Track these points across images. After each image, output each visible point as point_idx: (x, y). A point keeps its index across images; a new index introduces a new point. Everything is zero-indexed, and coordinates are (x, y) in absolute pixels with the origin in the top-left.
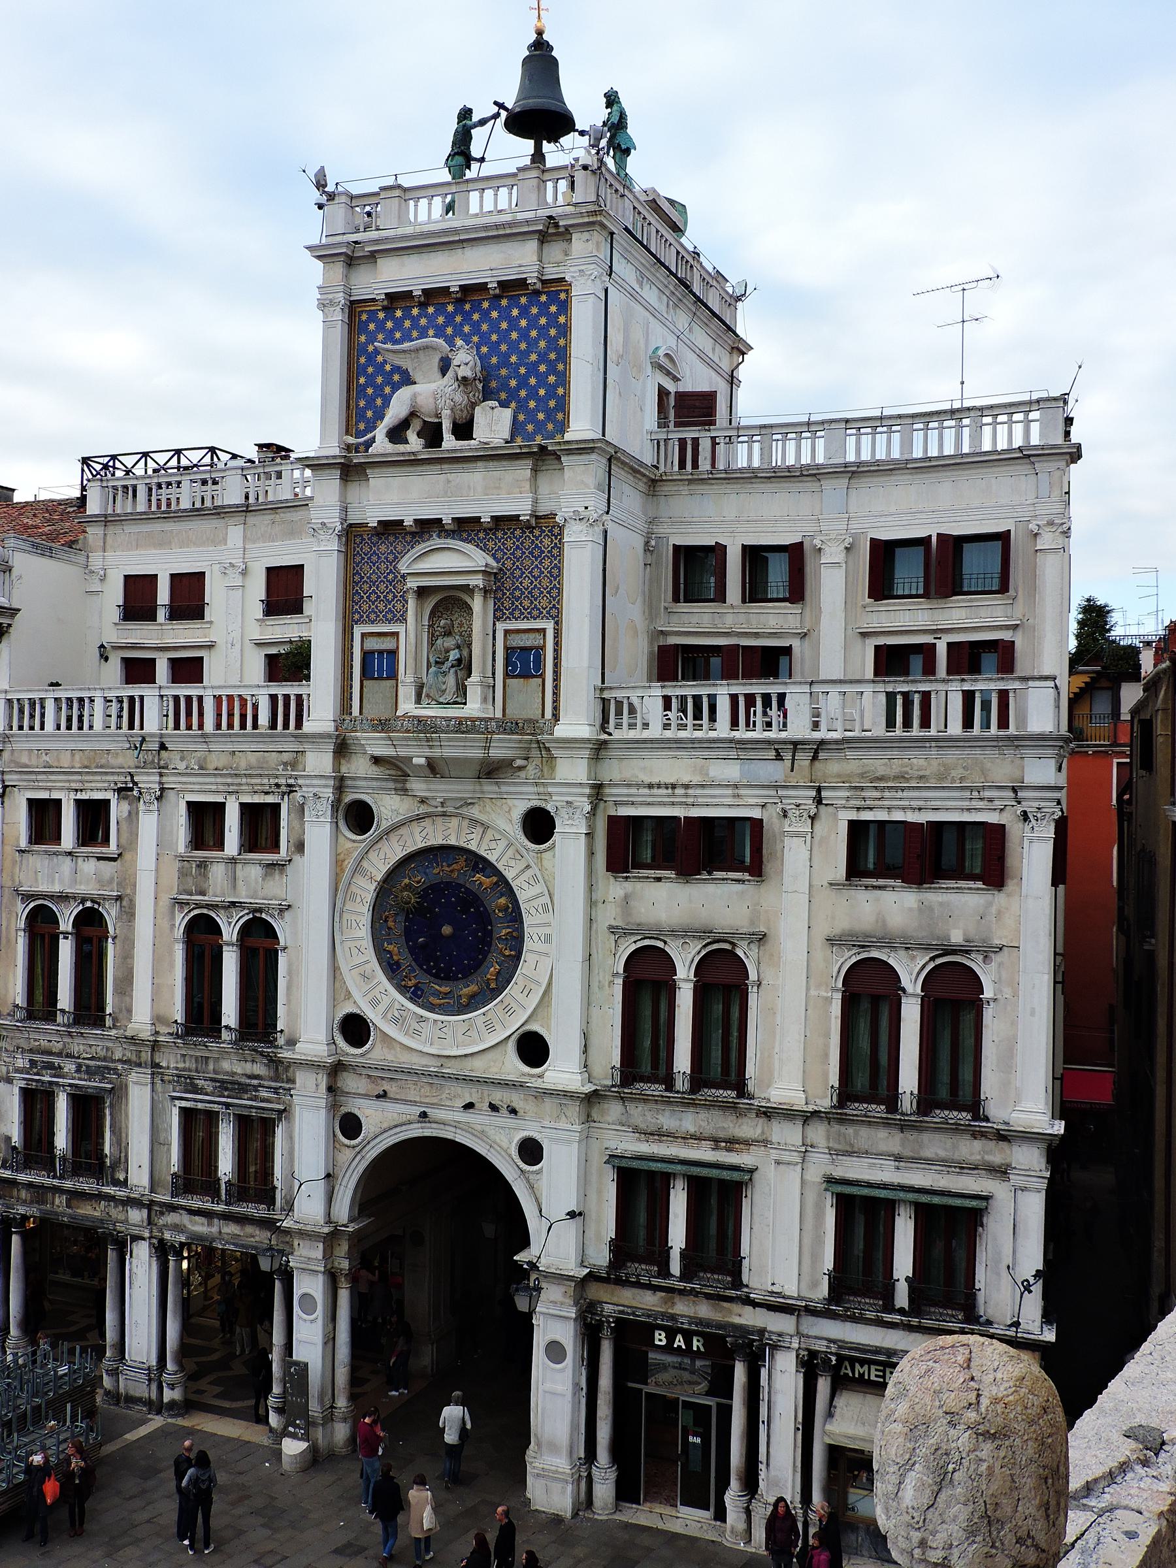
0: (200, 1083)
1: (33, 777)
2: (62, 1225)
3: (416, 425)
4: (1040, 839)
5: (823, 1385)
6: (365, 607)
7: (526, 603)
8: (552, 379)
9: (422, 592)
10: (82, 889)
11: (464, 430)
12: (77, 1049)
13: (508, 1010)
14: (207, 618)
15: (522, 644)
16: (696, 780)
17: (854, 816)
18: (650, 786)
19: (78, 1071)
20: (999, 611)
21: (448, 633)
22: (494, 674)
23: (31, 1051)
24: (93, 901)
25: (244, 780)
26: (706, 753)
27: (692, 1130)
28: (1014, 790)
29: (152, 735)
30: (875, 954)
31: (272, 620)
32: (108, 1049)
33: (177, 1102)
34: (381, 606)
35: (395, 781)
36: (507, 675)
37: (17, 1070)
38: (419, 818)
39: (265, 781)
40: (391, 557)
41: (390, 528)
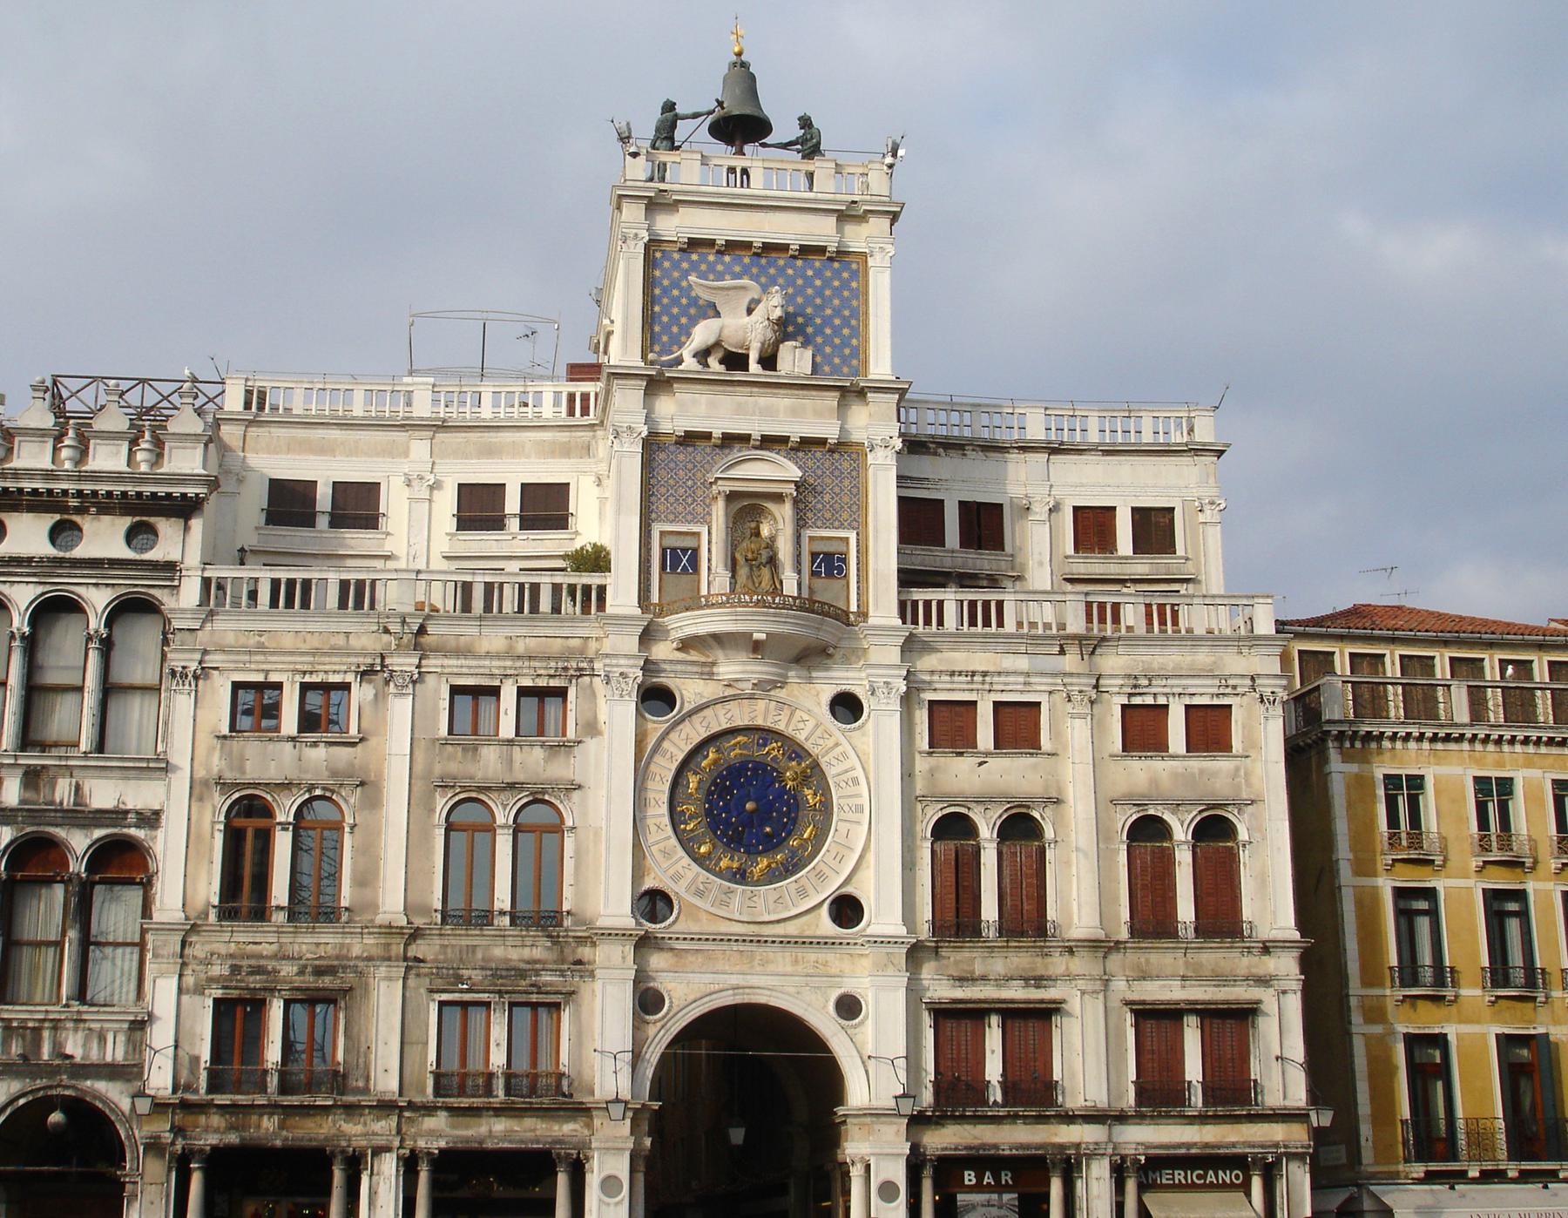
0: (466, 973)
1: (247, 658)
2: (274, 1151)
3: (720, 354)
4: (1274, 717)
6: (662, 508)
9: (731, 497)
10: (309, 778)
11: (769, 362)
13: (820, 876)
15: (825, 550)
18: (952, 674)
19: (301, 972)
23: (232, 956)
24: (324, 789)
26: (1000, 648)
27: (1003, 972)
28: (1253, 679)
29: (410, 615)
30: (1151, 812)
32: (342, 945)
34: (680, 509)
37: (211, 980)
38: (723, 700)
39: (553, 664)
40: (690, 466)
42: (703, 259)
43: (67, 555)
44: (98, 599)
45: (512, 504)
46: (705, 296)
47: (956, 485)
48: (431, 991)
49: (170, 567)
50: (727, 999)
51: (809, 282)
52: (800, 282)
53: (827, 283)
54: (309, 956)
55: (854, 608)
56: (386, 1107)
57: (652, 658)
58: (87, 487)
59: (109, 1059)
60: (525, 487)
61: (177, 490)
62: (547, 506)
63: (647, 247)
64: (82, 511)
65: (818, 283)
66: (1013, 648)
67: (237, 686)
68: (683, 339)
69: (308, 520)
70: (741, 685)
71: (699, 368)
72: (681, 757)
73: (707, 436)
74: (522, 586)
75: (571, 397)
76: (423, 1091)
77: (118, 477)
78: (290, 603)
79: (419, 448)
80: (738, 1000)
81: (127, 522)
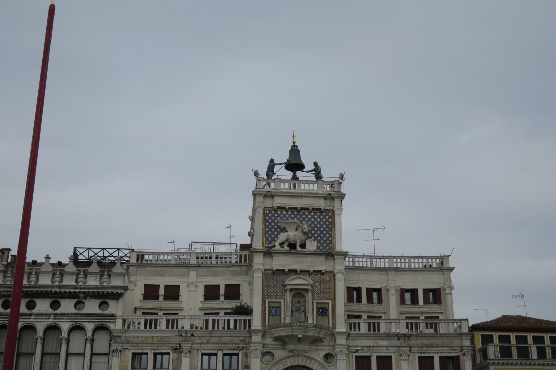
3: (287, 243)
4: (468, 360)
6: (269, 294)
7: (322, 295)
8: (328, 235)
9: (291, 290)
11: (303, 246)
16: (376, 345)
17: (420, 355)
20: (437, 309)
21: (299, 302)
22: (313, 314)
25: (226, 346)
26: (378, 338)
28: (461, 347)
31: (207, 302)
35: (282, 345)
36: (317, 316)
38: (289, 357)
42: (282, 213)
43: (80, 312)
44: (89, 327)
45: (222, 291)
46: (283, 225)
47: (365, 282)
49: (113, 315)
51: (316, 220)
52: (313, 220)
53: (321, 220)
55: (331, 326)
57: (266, 342)
58: (86, 291)
60: (226, 286)
61: (115, 291)
62: (233, 292)
63: (264, 210)
64: (85, 298)
65: (319, 220)
66: (383, 338)
67: (134, 355)
68: (276, 239)
69: (156, 298)
70: (295, 352)
71: (281, 249)
73: (283, 270)
74: (225, 320)
75: (241, 256)
77: (97, 287)
78: (151, 327)
79: (193, 274)
81: (99, 301)
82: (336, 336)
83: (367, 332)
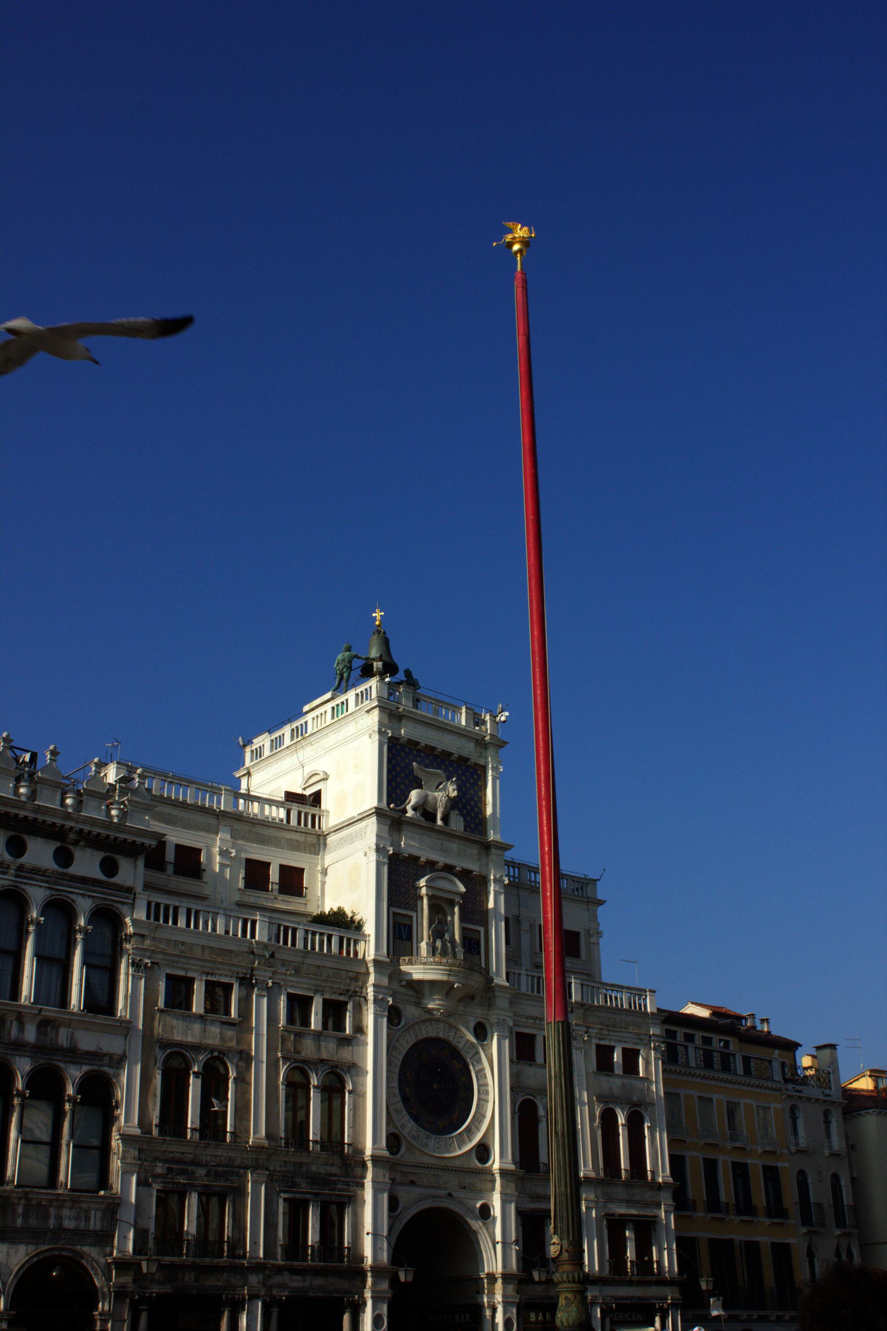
0: (298, 1180)
5: (608, 1320)
12: (204, 1158)
14: (205, 879)
17: (597, 1042)
19: (208, 1174)
31: (250, 892)
32: (230, 1158)
33: (282, 1195)
37: (156, 1176)
41: (415, 859)
48: (279, 1193)
49: (130, 890)
50: (428, 1204)
54: (212, 1163)
56: (259, 1267)
59: (92, 1227)
61: (139, 840)
64: (76, 843)
72: (404, 1052)
73: (417, 859)
76: (276, 1259)
80: (434, 1205)
82: (497, 994)
83: (530, 992)
